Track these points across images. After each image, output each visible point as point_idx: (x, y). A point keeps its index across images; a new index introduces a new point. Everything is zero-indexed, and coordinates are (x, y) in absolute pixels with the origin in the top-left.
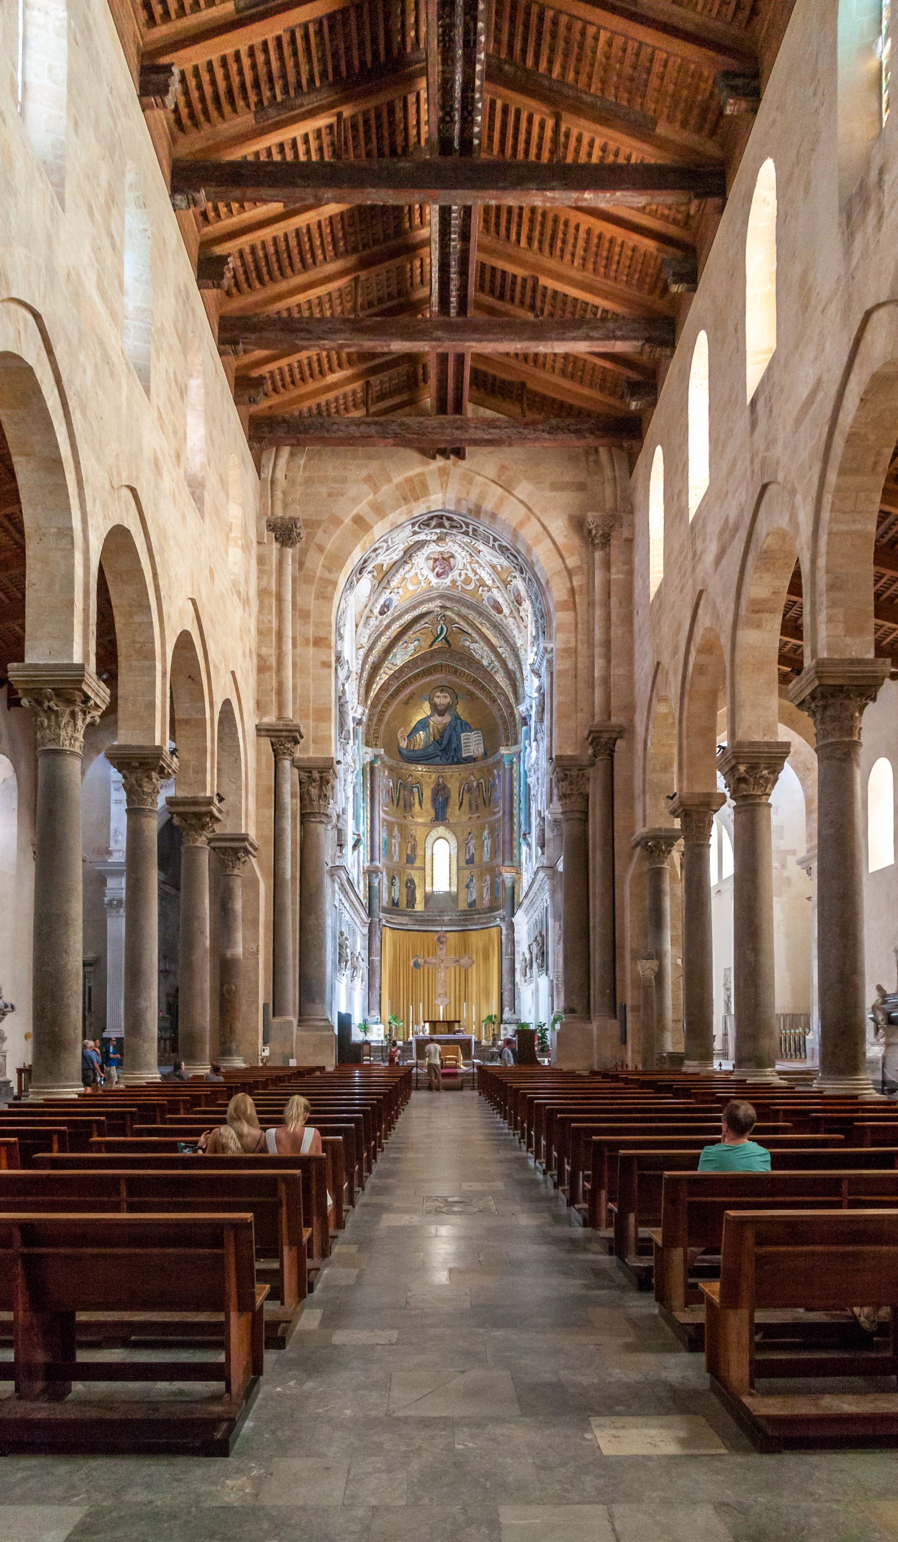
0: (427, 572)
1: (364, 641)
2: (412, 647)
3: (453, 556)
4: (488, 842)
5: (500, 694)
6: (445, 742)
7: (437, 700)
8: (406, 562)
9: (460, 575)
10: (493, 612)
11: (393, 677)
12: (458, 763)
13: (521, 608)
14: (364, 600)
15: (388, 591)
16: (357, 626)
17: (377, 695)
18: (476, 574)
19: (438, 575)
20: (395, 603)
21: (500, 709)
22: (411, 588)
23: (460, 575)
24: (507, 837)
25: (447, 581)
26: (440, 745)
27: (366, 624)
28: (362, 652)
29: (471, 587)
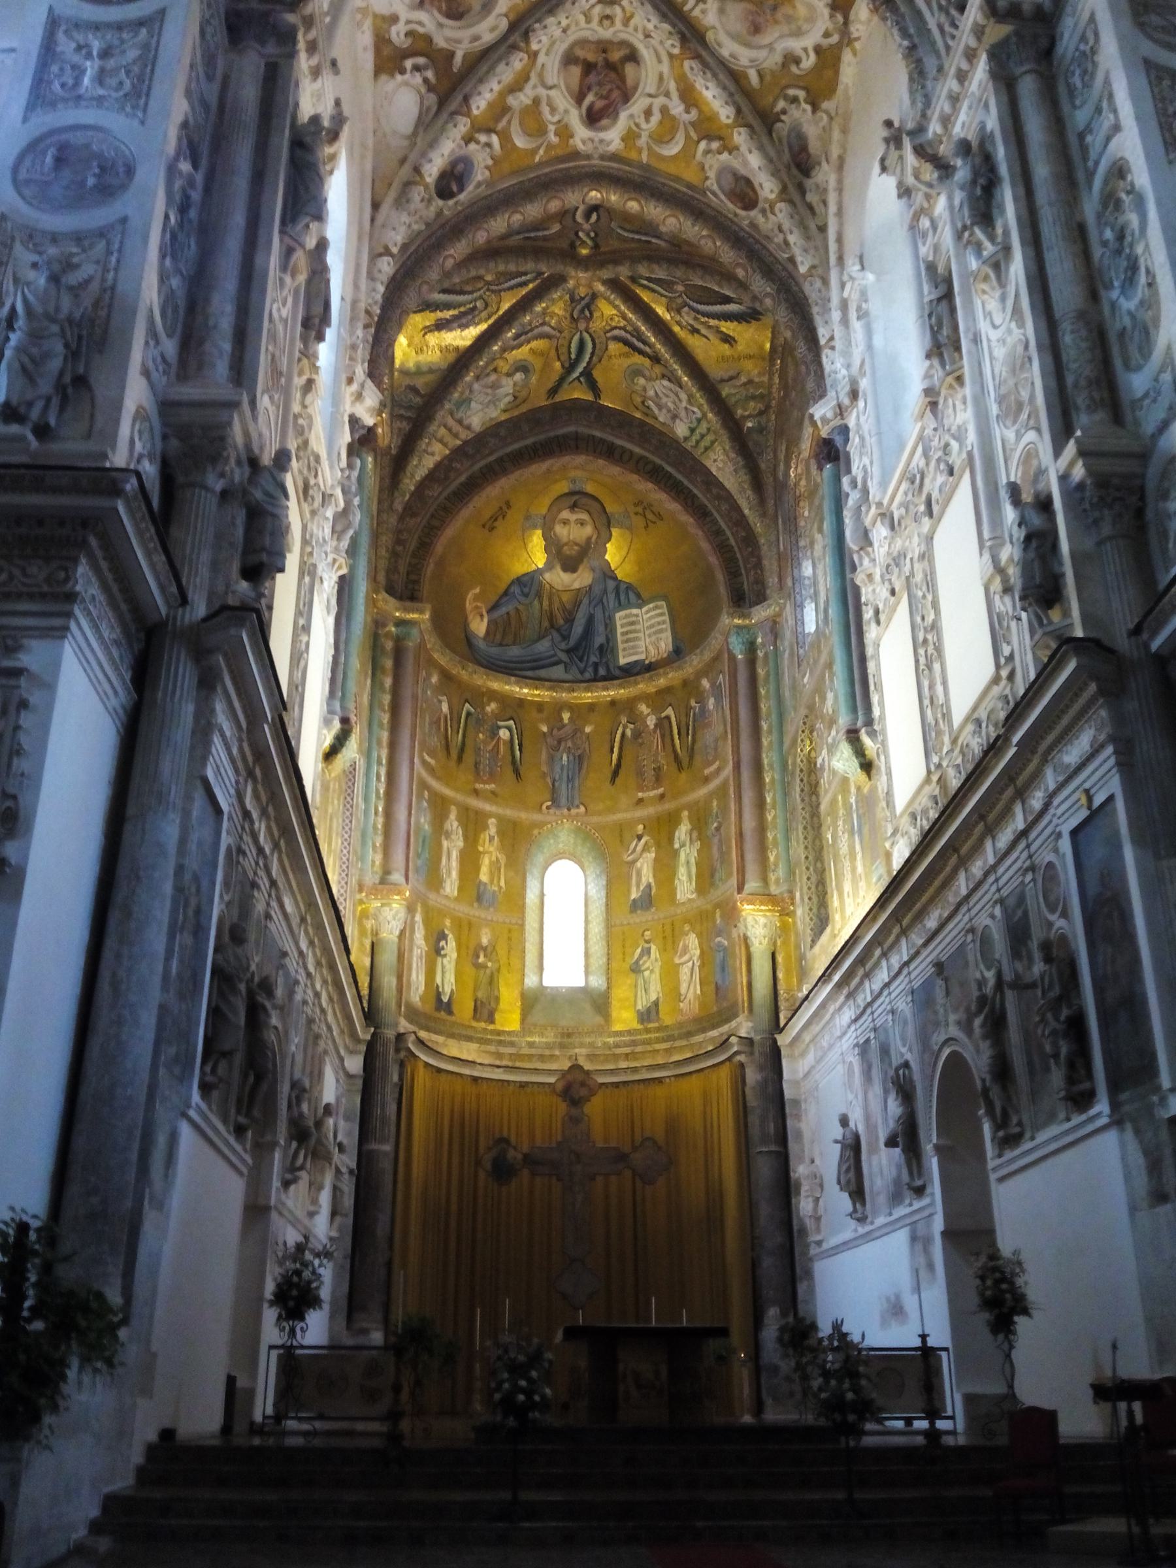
0: (562, 101)
1: (396, 238)
2: (508, 386)
3: (633, 57)
4: (688, 854)
5: (718, 497)
6: (578, 629)
7: (561, 531)
8: (514, 47)
9: (648, 113)
10: (730, 207)
11: (459, 453)
12: (609, 678)
13: (809, 183)
14: (398, 144)
15: (463, 126)
16: (376, 206)
17: (422, 485)
18: (688, 96)
19: (593, 118)
20: (480, 174)
21: (719, 532)
22: (520, 142)
23: (648, 113)
24: (749, 823)
25: (613, 137)
26: (565, 638)
27: (401, 201)
28: (387, 267)
29: (673, 149)
